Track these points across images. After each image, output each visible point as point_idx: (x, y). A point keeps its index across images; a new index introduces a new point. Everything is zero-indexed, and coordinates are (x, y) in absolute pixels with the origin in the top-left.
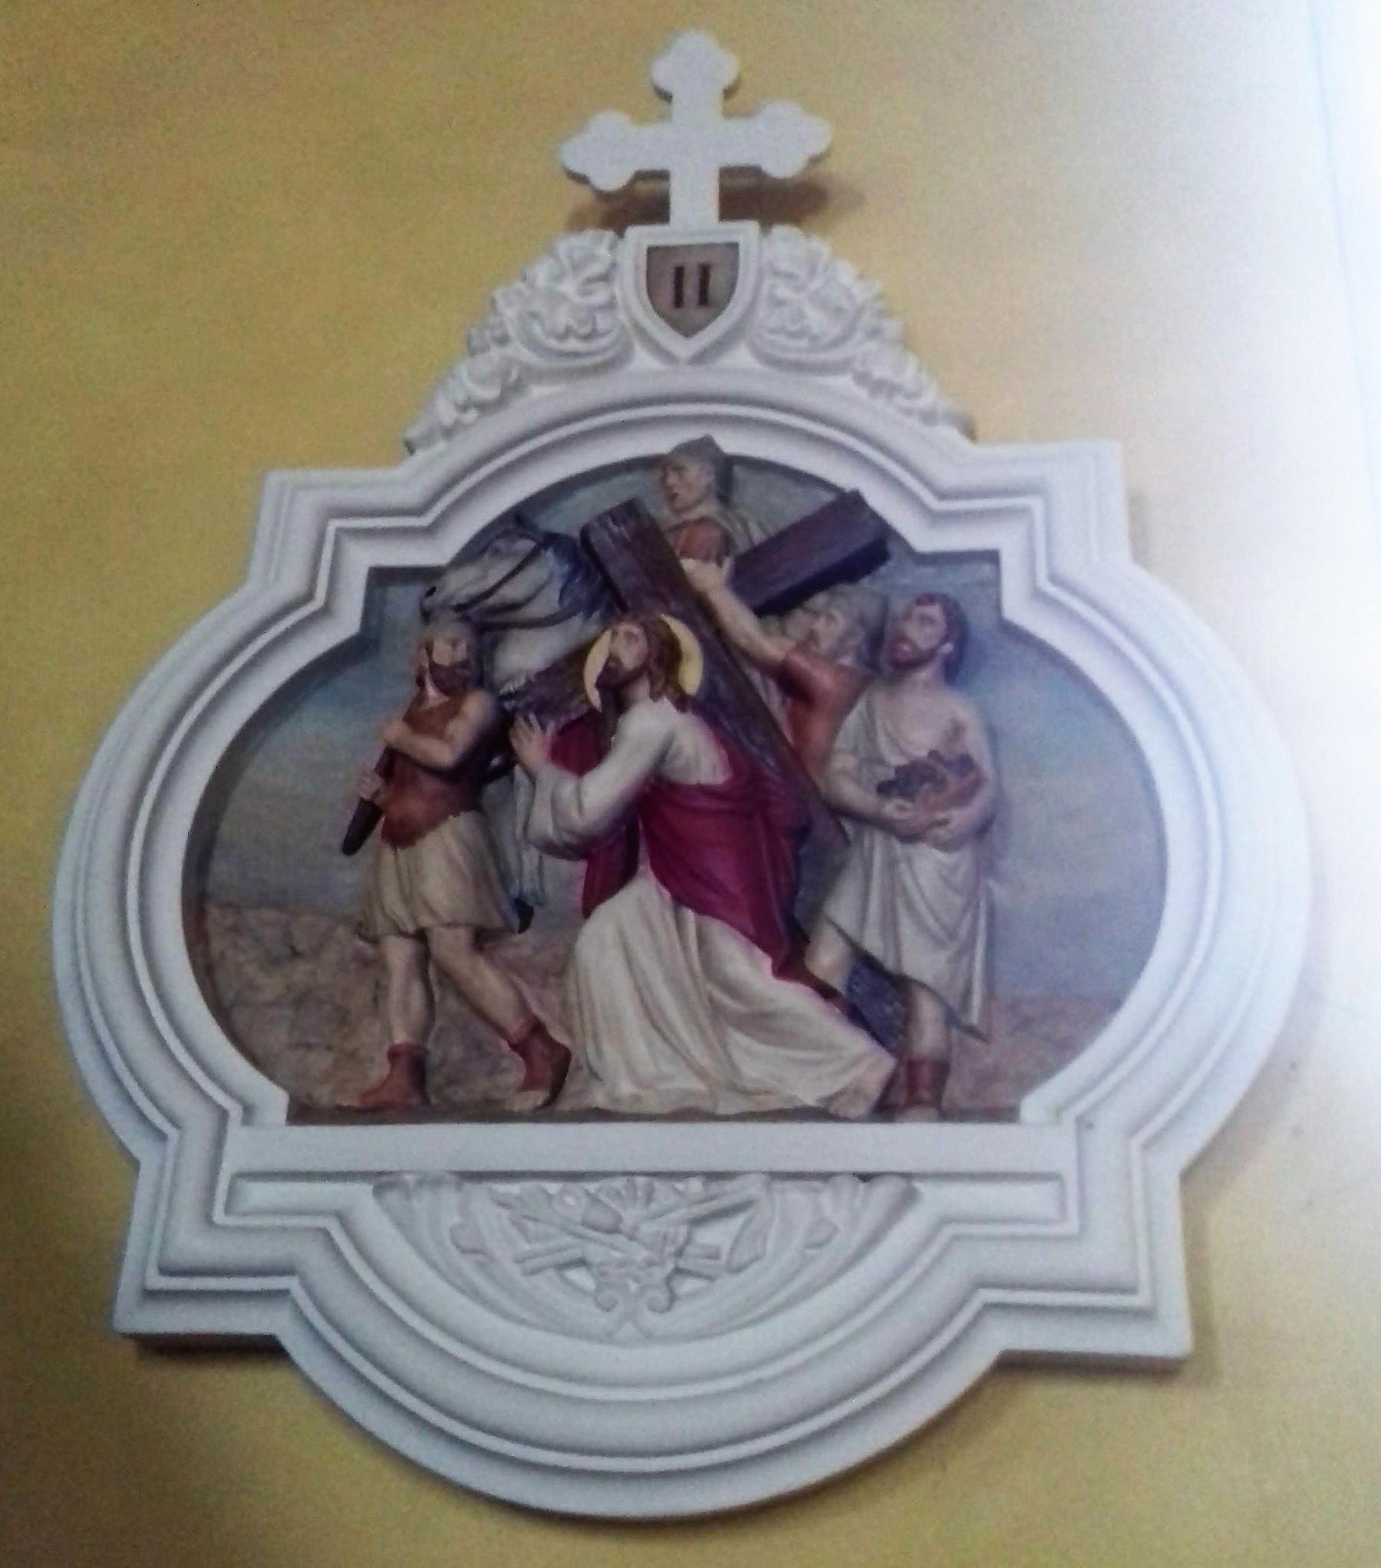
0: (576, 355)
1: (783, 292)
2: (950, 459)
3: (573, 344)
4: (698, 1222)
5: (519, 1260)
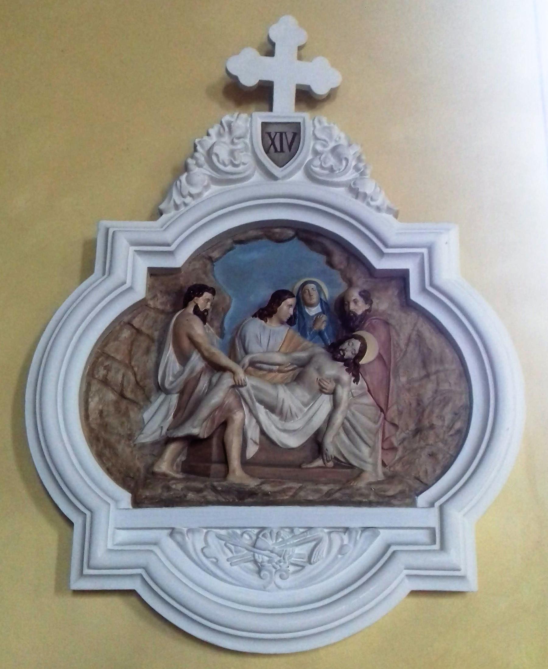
0: (232, 174)
1: (319, 148)
2: (390, 227)
3: (230, 168)
4: (297, 545)
5: (228, 560)
